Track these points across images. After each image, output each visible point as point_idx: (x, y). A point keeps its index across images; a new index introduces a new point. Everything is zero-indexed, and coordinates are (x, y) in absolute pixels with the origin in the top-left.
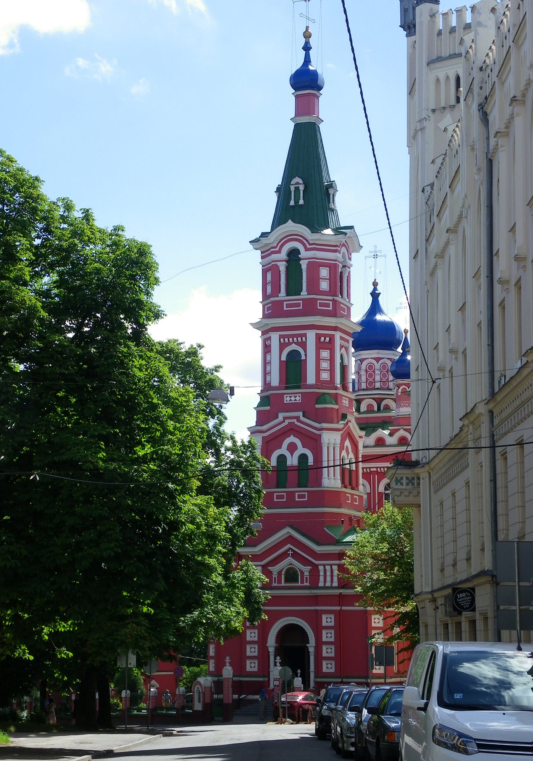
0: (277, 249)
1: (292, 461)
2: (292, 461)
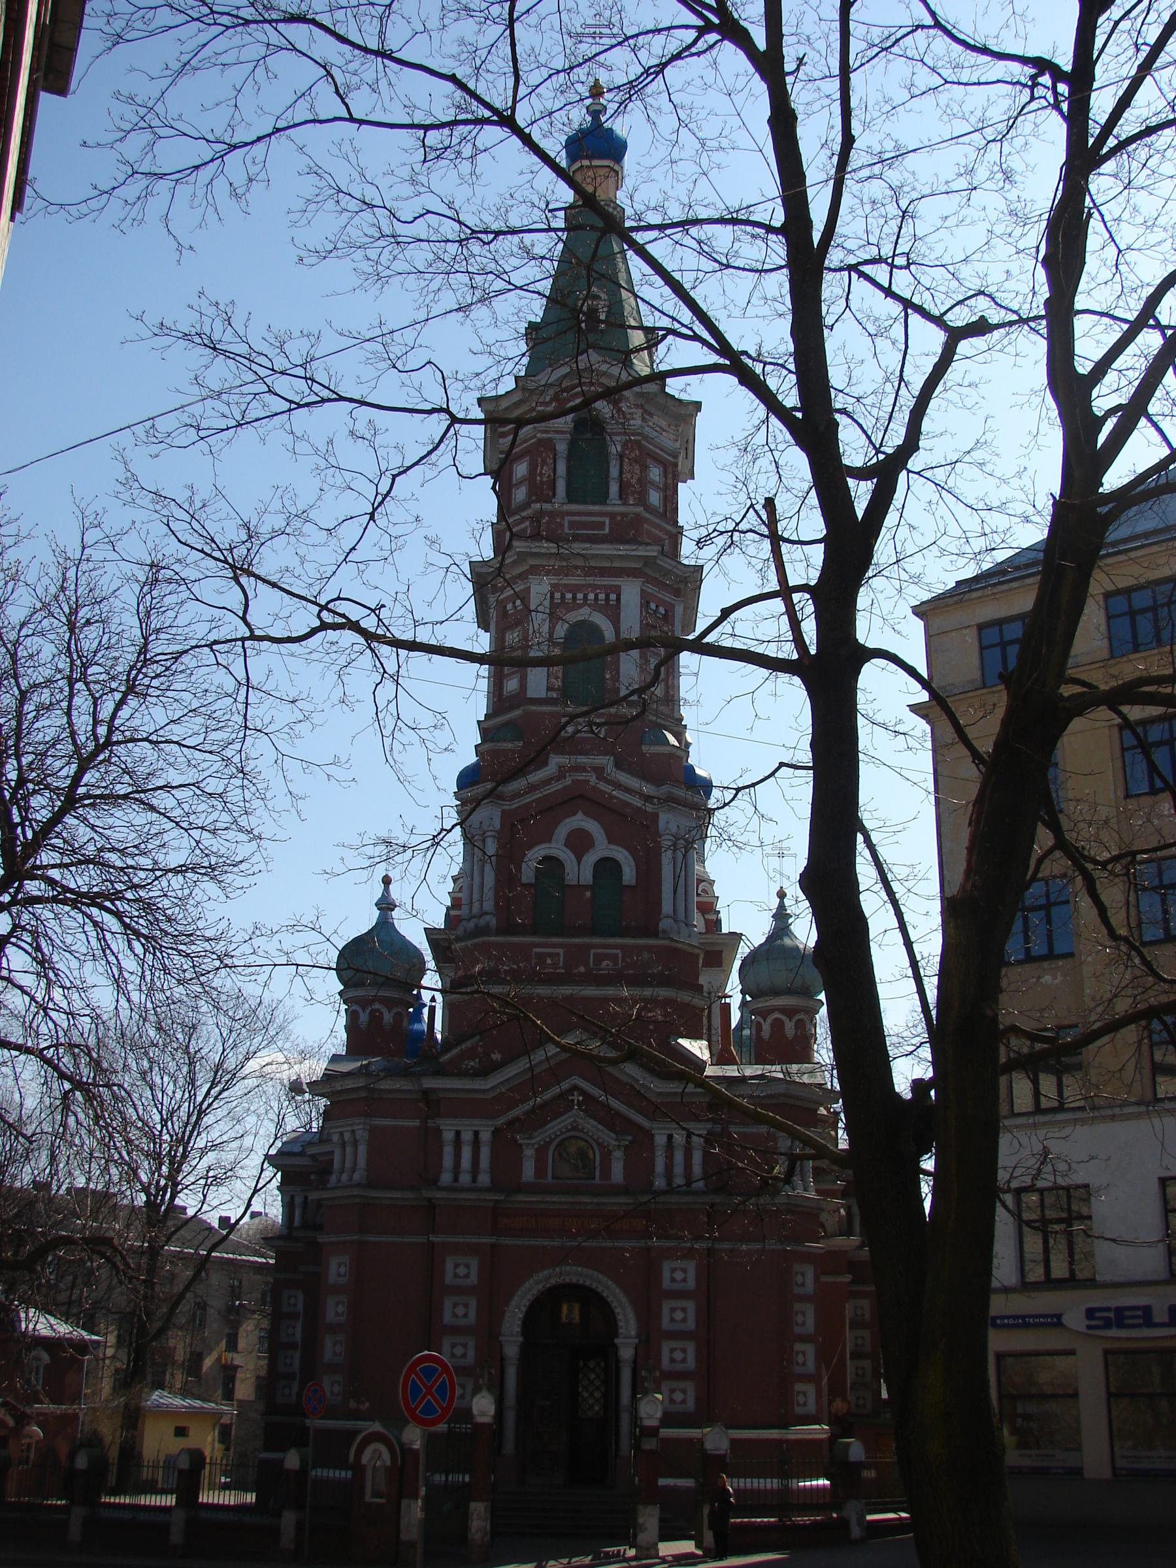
1: (579, 872)
2: (579, 872)
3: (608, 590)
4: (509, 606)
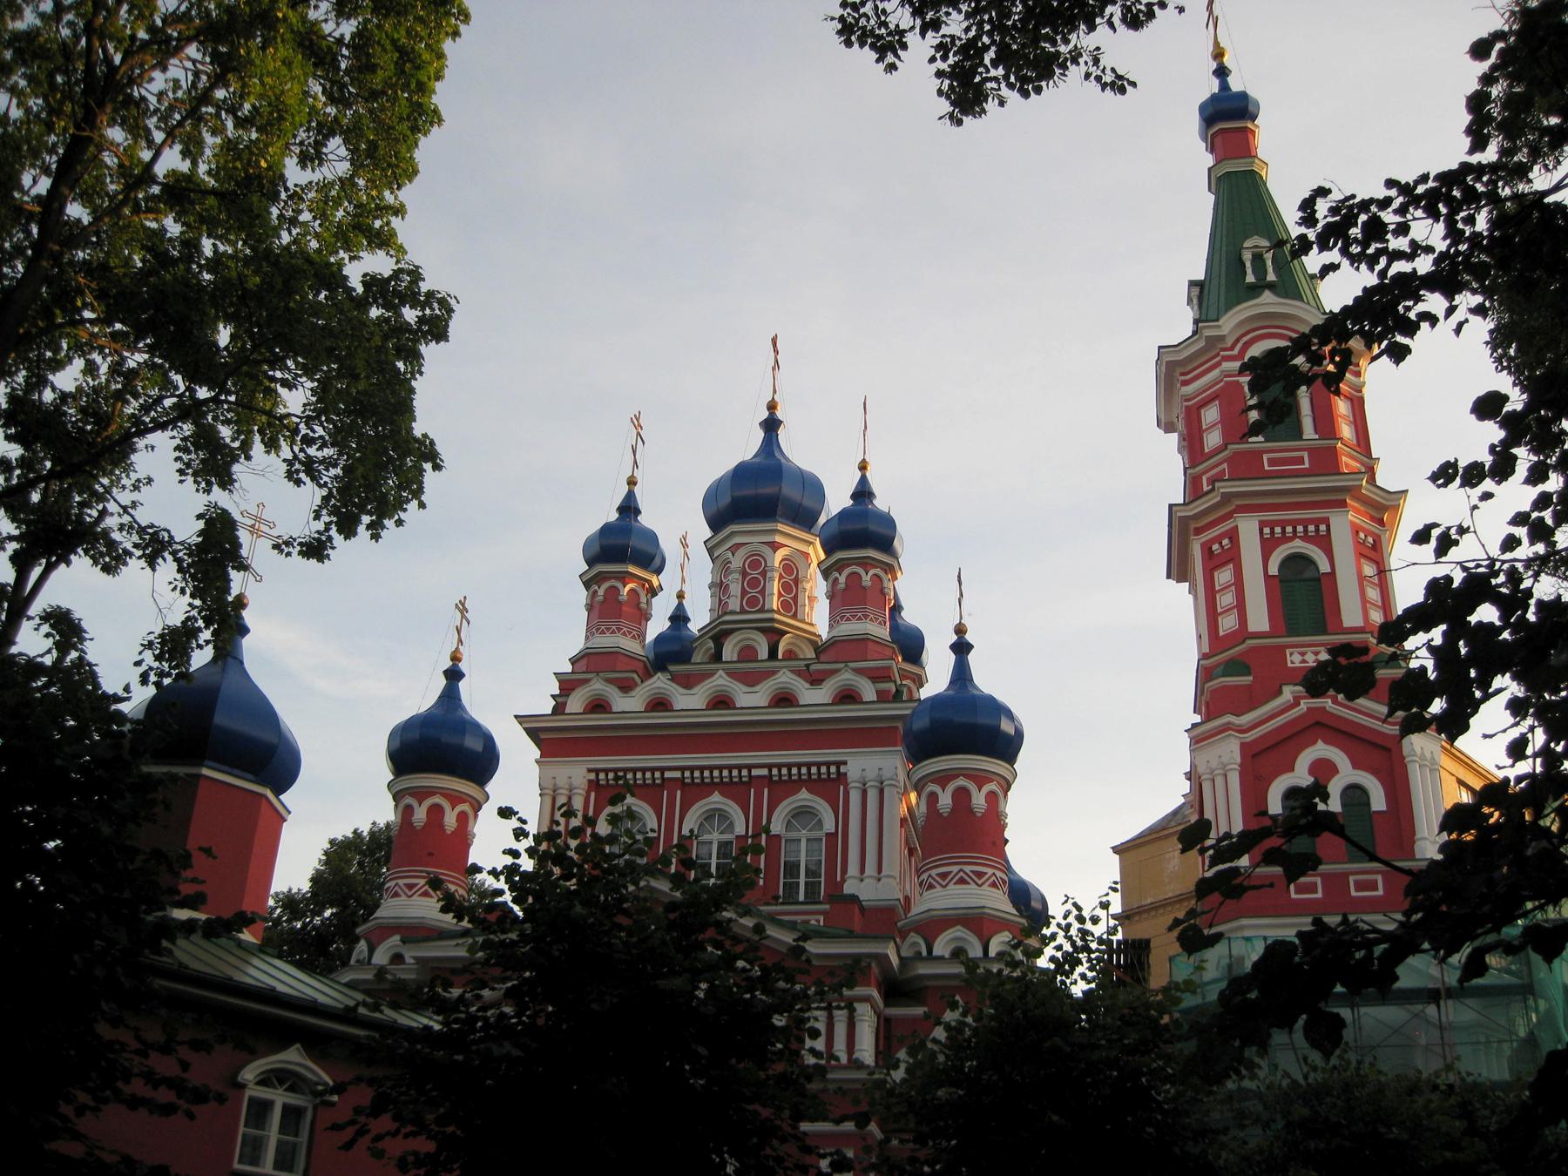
0: (1236, 352)
3: (1317, 522)
4: (1215, 547)
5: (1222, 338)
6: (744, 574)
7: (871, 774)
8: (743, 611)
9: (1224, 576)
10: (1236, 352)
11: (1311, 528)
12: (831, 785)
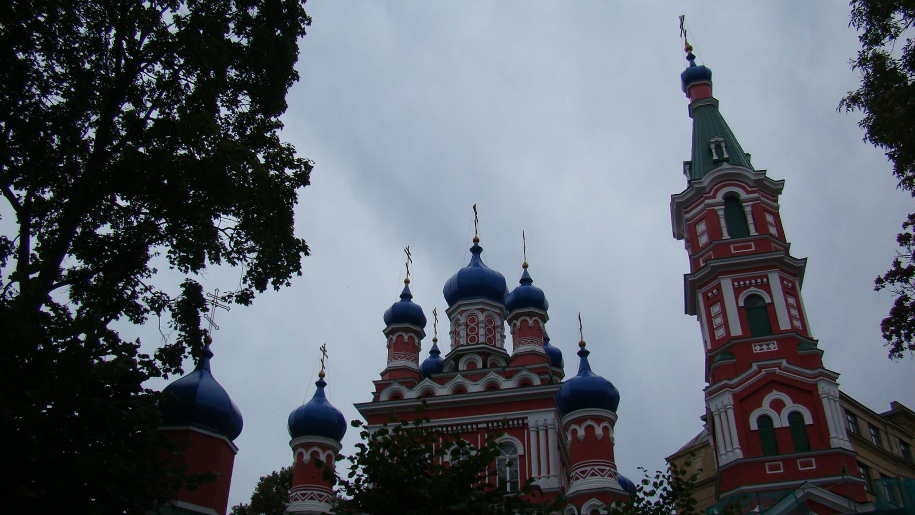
0: (711, 194)
1: (780, 421)
2: (780, 421)
3: (762, 277)
4: (710, 294)
5: (704, 188)
6: (467, 325)
7: (541, 422)
8: (468, 345)
9: (716, 309)
10: (711, 194)
11: (759, 281)
12: (520, 430)
